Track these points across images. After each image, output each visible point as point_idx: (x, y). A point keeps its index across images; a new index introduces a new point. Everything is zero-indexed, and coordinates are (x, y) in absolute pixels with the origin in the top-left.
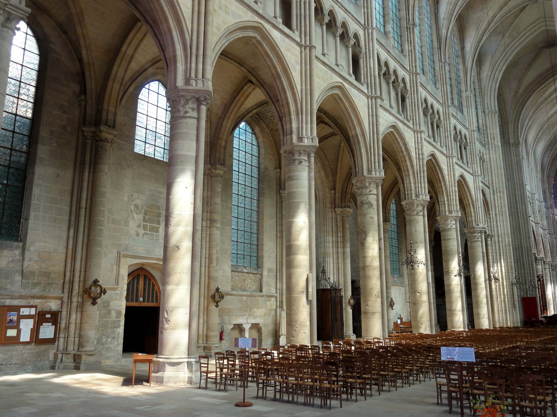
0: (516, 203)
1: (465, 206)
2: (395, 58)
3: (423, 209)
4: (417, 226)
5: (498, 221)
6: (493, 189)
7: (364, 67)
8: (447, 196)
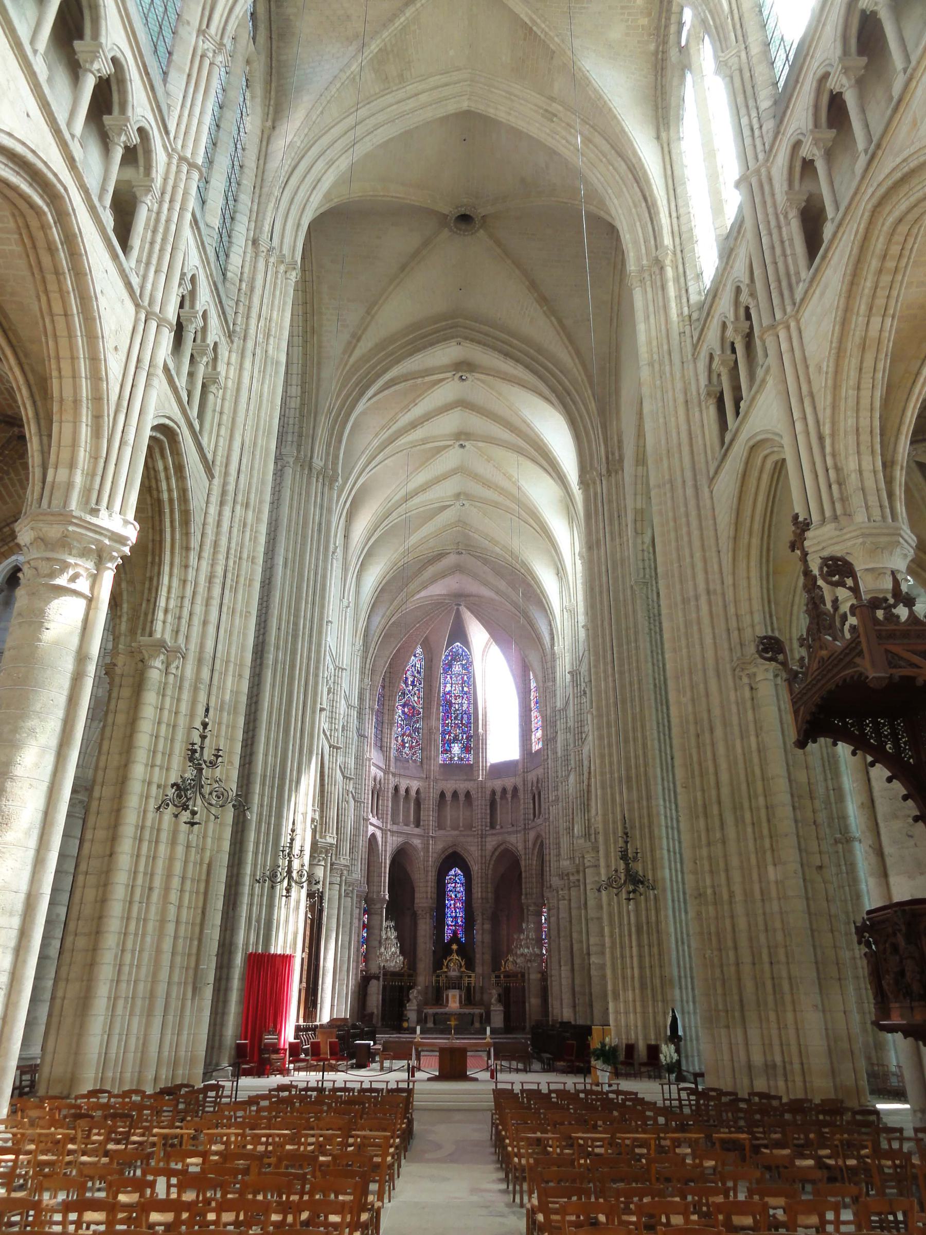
0: (295, 637)
1: (55, 408)
5: (215, 602)
6: (225, 484)
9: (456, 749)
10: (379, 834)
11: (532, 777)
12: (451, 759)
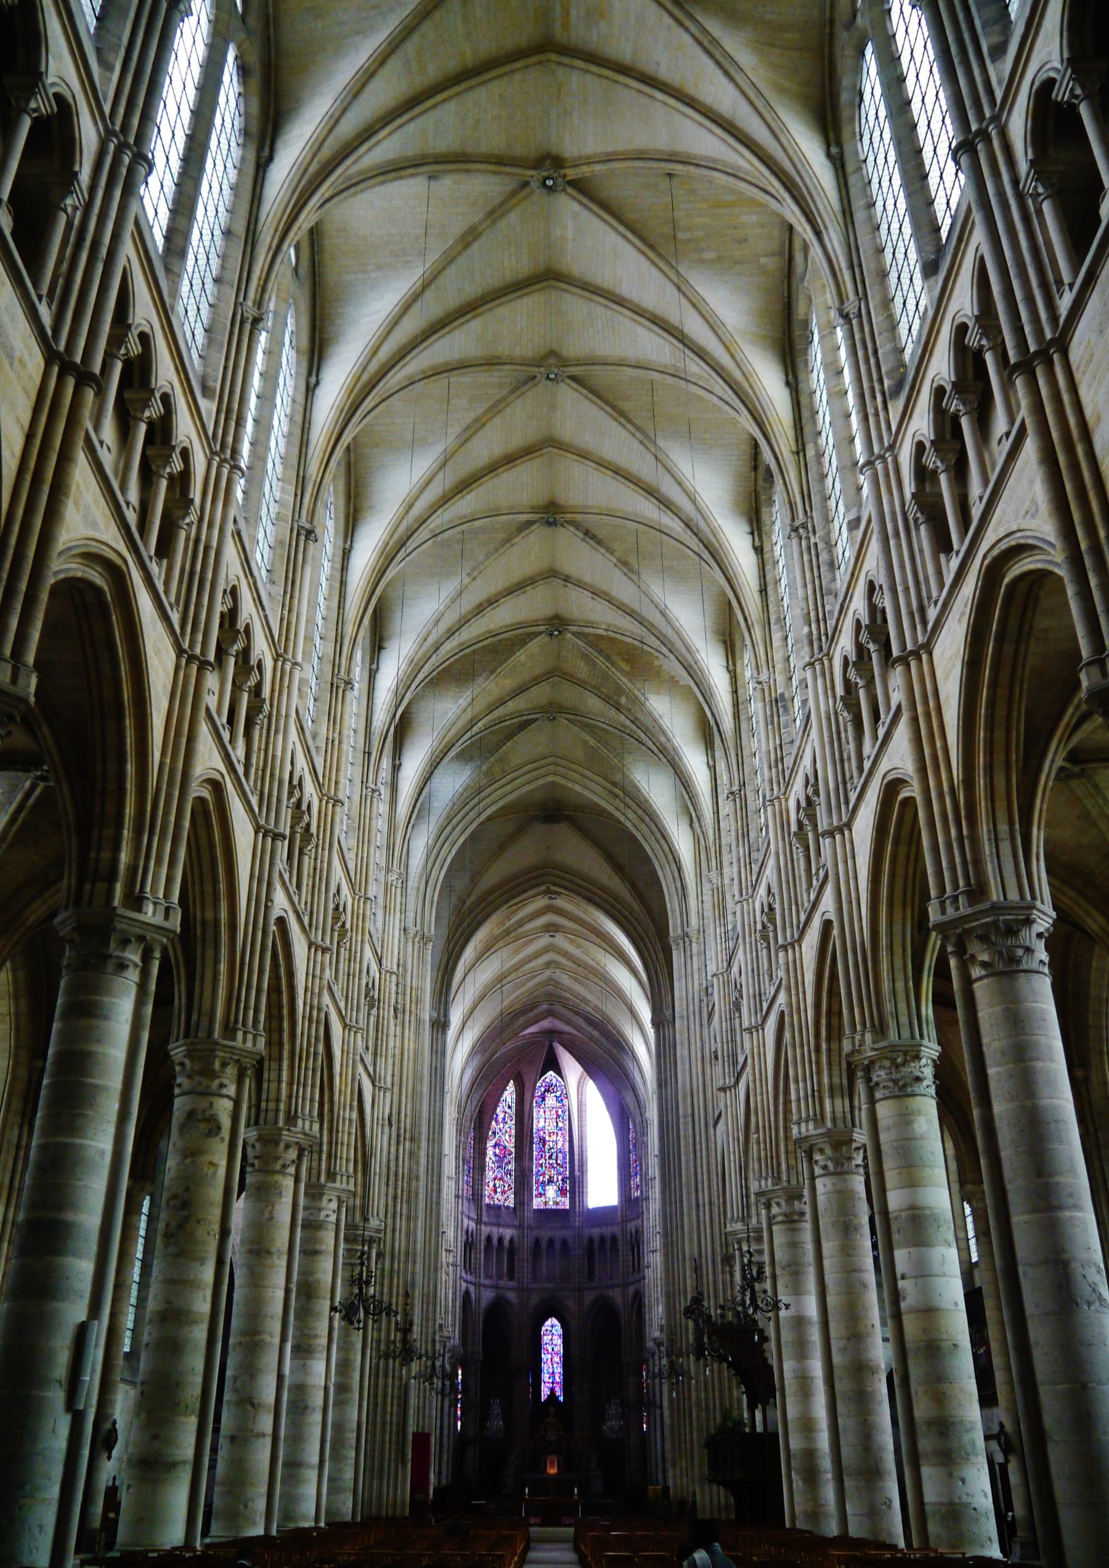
2: (308, 748)
3: (300, 1157)
4: (277, 1207)
5: (398, 1216)
6: (399, 1129)
7: (259, 749)
8: (330, 1131)
9: (551, 1191)
10: (472, 1289)
11: (631, 1226)
12: (546, 1203)
